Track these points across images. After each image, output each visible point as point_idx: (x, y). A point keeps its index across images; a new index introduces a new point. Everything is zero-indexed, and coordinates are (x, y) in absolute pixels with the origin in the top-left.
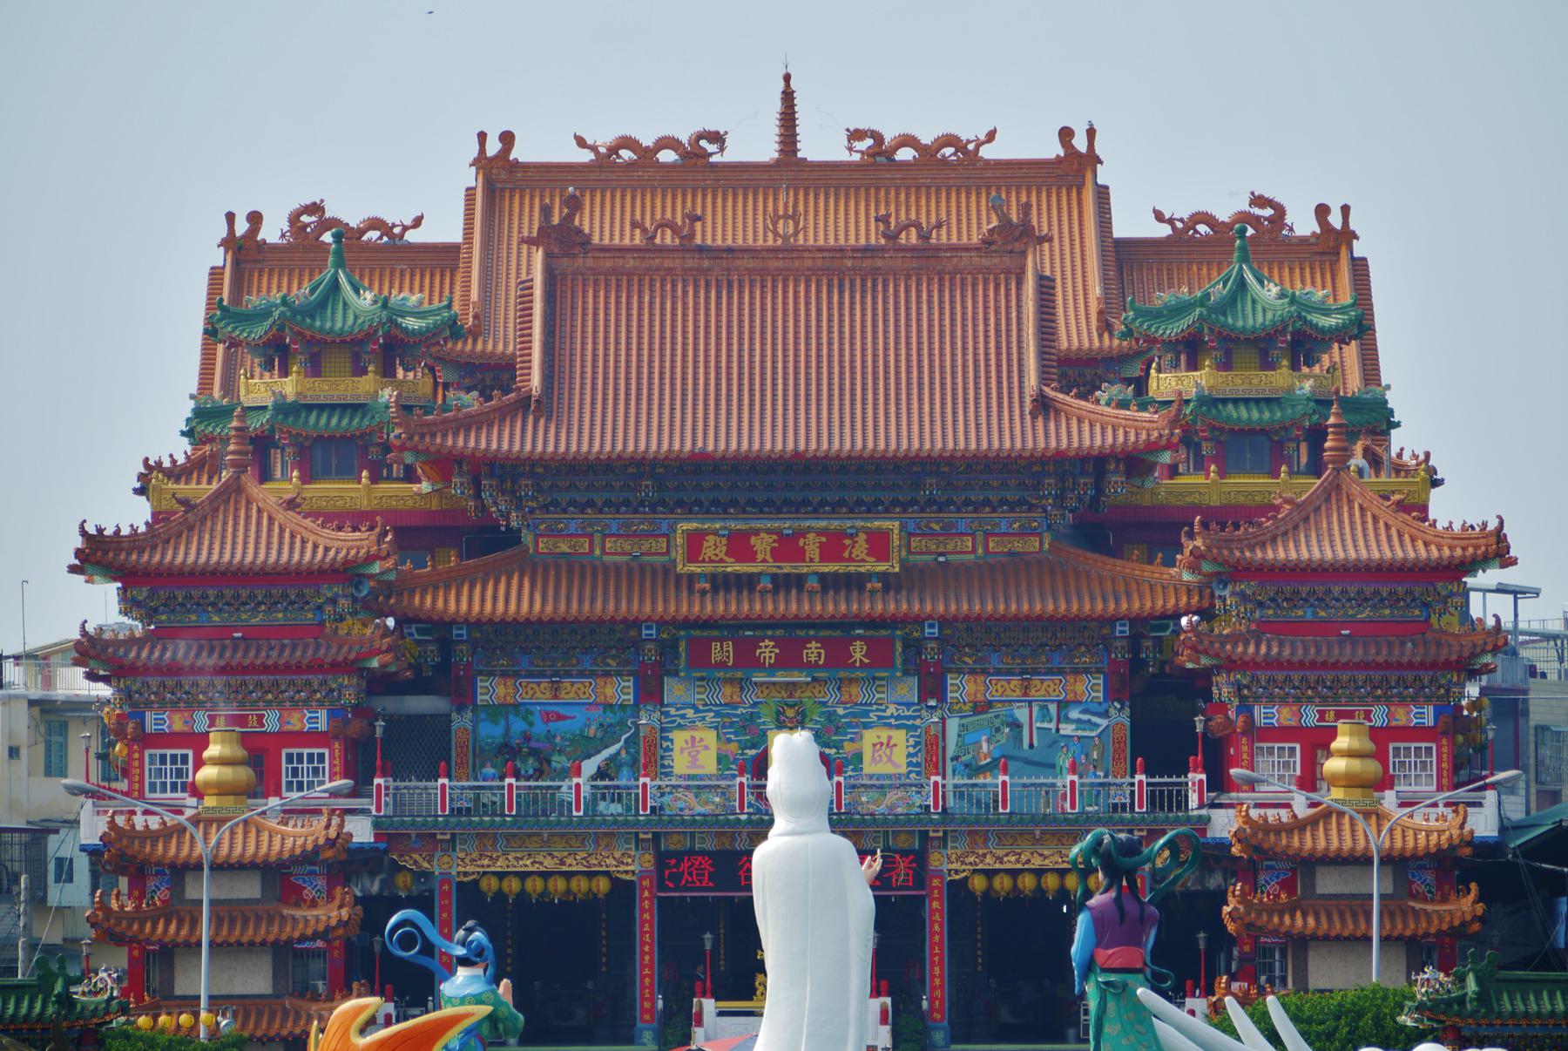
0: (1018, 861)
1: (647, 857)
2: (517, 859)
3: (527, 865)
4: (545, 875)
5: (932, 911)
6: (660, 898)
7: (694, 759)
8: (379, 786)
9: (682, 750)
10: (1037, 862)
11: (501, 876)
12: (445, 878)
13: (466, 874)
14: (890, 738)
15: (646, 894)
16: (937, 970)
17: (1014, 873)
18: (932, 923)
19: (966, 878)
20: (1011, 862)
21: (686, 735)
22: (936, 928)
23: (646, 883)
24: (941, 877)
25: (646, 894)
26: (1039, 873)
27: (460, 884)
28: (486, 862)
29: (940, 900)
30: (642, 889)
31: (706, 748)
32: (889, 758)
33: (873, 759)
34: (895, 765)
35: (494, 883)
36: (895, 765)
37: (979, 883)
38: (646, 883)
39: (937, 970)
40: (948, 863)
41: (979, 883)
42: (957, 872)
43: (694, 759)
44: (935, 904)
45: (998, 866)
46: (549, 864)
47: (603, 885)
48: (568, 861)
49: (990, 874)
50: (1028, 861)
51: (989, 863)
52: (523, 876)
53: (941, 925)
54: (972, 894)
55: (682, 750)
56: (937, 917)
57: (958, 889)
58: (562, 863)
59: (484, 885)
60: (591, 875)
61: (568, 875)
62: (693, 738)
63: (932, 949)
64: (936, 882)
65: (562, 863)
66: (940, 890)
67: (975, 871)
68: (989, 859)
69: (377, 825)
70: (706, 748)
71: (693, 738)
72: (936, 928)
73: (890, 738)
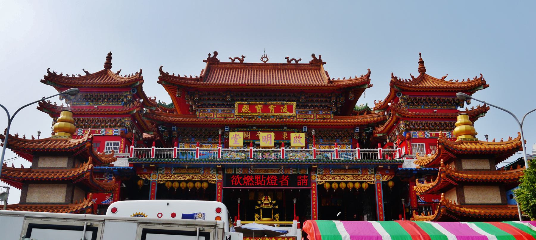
0: (340, 179)
1: (220, 176)
2: (178, 176)
3: (181, 178)
4: (187, 182)
5: (313, 194)
6: (224, 189)
7: (236, 141)
8: (132, 148)
9: (232, 138)
10: (346, 179)
11: (172, 182)
12: (154, 182)
13: (161, 181)
14: (299, 135)
15: (219, 188)
16: (315, 213)
17: (339, 183)
18: (313, 198)
19: (323, 184)
20: (337, 179)
21: (233, 133)
22: (314, 199)
23: (219, 184)
24: (315, 183)
25: (219, 188)
26: (347, 182)
27: (159, 185)
28: (168, 177)
29: (315, 190)
30: (218, 186)
31: (240, 138)
32: (299, 141)
33: (294, 142)
34: (301, 143)
35: (170, 184)
36: (301, 143)
37: (327, 185)
38: (219, 184)
39: (315, 213)
40: (317, 179)
41: (327, 185)
42: (320, 182)
43: (236, 141)
44: (314, 192)
45: (333, 180)
46: (188, 178)
47: (205, 185)
48: (195, 177)
49: (331, 183)
50: (343, 179)
51: (331, 179)
52: (179, 182)
53: (316, 198)
54: (325, 189)
55: (232, 138)
56: (314, 196)
57: (321, 187)
58: (193, 178)
59: (167, 184)
60: (201, 182)
61: (194, 182)
62: (236, 135)
63: (313, 206)
64: (314, 185)
65: (193, 178)
66: (315, 187)
67: (326, 182)
68: (330, 178)
69: (129, 160)
70: (240, 138)
71: (236, 135)
72: (314, 199)
73: (299, 135)
